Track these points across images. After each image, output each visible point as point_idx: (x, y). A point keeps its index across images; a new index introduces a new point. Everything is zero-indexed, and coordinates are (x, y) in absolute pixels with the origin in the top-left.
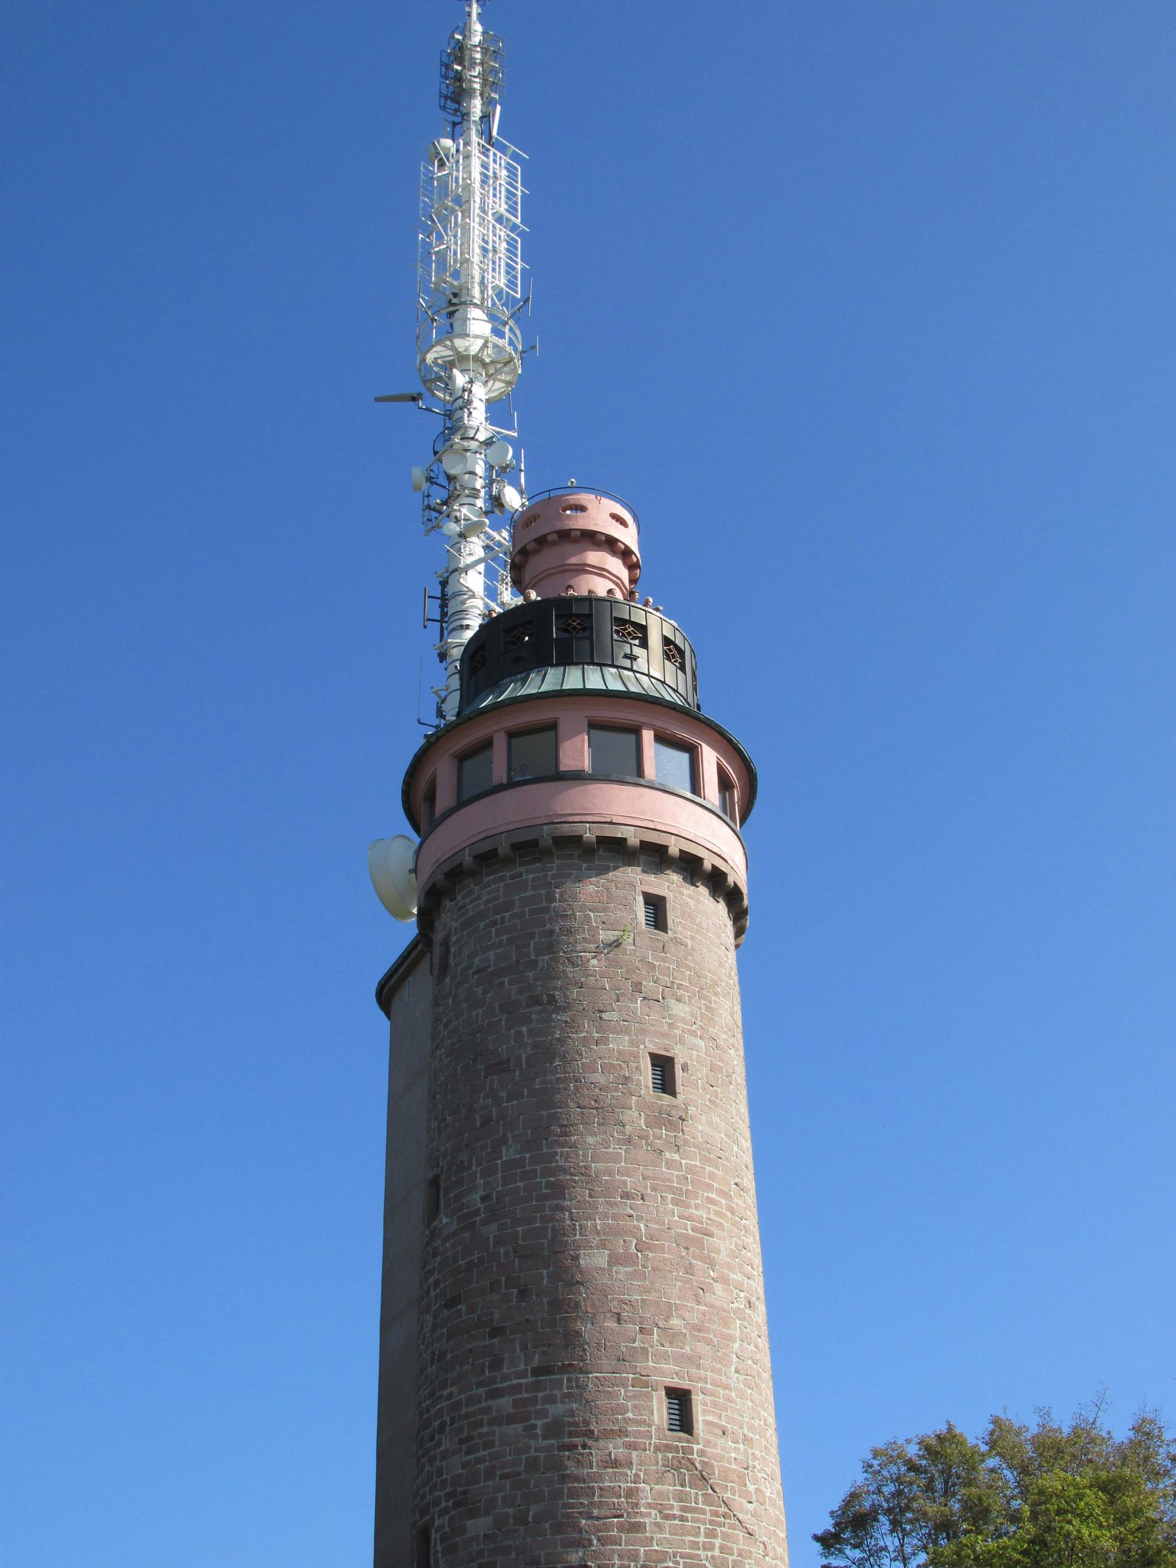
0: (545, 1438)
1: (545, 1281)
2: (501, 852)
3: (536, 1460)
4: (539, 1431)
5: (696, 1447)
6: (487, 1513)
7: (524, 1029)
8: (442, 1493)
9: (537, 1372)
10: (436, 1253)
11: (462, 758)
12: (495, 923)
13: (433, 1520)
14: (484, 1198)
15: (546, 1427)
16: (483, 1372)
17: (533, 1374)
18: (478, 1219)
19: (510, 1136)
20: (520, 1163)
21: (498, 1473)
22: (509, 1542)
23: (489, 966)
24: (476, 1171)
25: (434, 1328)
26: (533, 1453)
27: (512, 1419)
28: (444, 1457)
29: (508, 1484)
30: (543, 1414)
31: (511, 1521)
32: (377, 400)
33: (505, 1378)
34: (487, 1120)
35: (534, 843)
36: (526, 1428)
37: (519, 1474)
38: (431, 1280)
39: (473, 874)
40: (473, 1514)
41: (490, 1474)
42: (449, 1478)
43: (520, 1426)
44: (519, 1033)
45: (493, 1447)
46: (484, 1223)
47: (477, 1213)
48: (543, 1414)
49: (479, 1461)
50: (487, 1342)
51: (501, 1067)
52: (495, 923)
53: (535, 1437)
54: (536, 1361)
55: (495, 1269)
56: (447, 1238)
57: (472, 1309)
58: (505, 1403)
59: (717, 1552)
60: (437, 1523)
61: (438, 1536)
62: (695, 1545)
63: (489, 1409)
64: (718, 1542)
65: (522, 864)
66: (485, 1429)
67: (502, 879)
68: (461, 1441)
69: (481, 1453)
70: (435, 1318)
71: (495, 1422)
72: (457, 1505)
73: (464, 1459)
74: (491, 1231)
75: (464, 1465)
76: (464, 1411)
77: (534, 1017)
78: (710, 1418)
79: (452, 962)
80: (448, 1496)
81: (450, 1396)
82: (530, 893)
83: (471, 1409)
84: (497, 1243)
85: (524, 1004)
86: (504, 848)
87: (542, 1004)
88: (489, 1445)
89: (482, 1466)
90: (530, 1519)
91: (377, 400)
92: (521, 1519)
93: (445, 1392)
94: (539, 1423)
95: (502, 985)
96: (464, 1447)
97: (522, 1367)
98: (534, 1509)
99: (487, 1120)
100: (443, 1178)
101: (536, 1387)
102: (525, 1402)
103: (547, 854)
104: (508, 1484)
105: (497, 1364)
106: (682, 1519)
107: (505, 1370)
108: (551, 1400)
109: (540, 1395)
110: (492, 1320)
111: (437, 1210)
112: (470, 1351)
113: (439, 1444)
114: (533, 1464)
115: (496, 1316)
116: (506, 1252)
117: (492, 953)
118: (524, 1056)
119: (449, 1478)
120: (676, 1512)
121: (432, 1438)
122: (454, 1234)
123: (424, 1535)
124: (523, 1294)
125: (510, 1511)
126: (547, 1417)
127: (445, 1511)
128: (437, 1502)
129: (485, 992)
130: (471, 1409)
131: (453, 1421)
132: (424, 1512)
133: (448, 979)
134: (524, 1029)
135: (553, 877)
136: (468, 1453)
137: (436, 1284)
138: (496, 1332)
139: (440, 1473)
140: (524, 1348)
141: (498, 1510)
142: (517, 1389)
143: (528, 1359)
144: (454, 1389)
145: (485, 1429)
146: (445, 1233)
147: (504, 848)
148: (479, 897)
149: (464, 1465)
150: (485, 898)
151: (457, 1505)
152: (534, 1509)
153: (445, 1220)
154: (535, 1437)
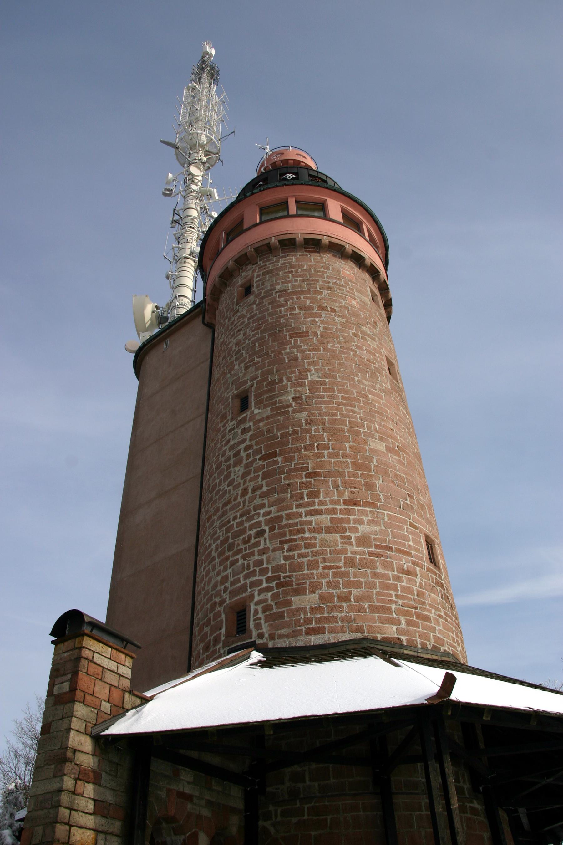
0: (358, 545)
7: (317, 320)
8: (263, 578)
10: (244, 431)
13: (252, 597)
14: (294, 399)
15: (358, 539)
16: (302, 498)
18: (290, 409)
21: (321, 565)
23: (289, 289)
24: (287, 384)
26: (349, 555)
27: (328, 530)
28: (263, 552)
30: (356, 530)
31: (336, 599)
32: (161, 141)
37: (340, 567)
40: (299, 591)
42: (270, 567)
43: (337, 536)
45: (315, 547)
46: (295, 411)
47: (290, 406)
48: (356, 530)
49: (301, 556)
53: (351, 544)
54: (346, 496)
55: (308, 438)
56: (262, 420)
58: (325, 519)
60: (257, 598)
61: (260, 608)
63: (310, 523)
66: (307, 535)
68: (282, 542)
69: (303, 551)
71: (318, 530)
72: (278, 586)
73: (285, 554)
75: (286, 558)
76: (284, 522)
81: (269, 513)
83: (291, 521)
87: (328, 311)
88: (307, 546)
89: (305, 560)
90: (352, 599)
91: (161, 141)
92: (345, 598)
94: (353, 536)
96: (286, 546)
97: (336, 498)
98: (355, 592)
101: (348, 512)
102: (341, 521)
105: (314, 494)
107: (322, 498)
108: (361, 522)
109: (352, 517)
110: (308, 467)
112: (289, 485)
113: (257, 544)
114: (350, 562)
116: (317, 430)
118: (318, 332)
119: (270, 567)
121: (246, 541)
122: (268, 418)
126: (358, 532)
128: (260, 582)
130: (291, 521)
131: (272, 529)
136: (289, 550)
138: (309, 475)
139: (260, 562)
142: (334, 511)
143: (340, 494)
145: (307, 535)
146: (258, 418)
149: (286, 558)
151: (278, 586)
152: (355, 592)
153: (256, 411)
154: (351, 544)
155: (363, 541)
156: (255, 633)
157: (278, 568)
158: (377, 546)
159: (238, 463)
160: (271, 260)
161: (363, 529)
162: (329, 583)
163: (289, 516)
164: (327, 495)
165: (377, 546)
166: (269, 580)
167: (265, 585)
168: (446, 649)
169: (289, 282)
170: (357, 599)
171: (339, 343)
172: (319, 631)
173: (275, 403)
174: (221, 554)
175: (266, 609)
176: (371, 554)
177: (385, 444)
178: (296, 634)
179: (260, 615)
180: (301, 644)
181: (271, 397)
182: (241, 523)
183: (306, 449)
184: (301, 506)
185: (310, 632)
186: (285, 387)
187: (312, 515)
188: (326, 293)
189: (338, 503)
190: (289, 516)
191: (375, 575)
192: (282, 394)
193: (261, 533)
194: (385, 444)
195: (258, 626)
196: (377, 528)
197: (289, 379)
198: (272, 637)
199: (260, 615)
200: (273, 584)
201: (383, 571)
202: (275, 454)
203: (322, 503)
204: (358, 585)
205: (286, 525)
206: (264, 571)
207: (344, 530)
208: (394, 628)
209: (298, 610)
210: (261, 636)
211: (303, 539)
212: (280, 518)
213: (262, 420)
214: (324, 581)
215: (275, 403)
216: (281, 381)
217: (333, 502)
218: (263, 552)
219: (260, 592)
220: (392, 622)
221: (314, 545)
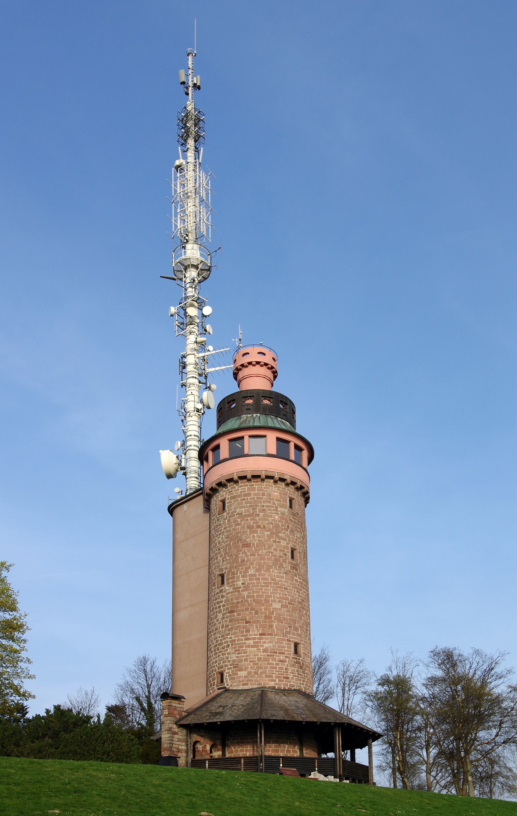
0: (263, 653)
1: (263, 610)
2: (248, 477)
3: (260, 658)
4: (261, 650)
5: (301, 658)
6: (245, 670)
7: (255, 535)
8: (229, 664)
9: (260, 635)
10: (223, 596)
11: (230, 440)
12: (244, 499)
13: (225, 670)
16: (243, 633)
17: (259, 635)
18: (240, 589)
19: (251, 567)
20: (255, 575)
21: (249, 660)
22: (252, 679)
23: (243, 513)
24: (240, 575)
25: (223, 618)
26: (259, 656)
27: (253, 646)
28: (229, 654)
29: (252, 663)
30: (262, 646)
31: (253, 673)
33: (251, 635)
34: (243, 561)
35: (259, 476)
36: (257, 649)
37: (255, 661)
38: (221, 604)
39: (236, 482)
40: (240, 670)
41: (246, 660)
42: (231, 660)
44: (253, 536)
45: (247, 653)
46: (243, 591)
47: (240, 587)
48: (262, 646)
49: (242, 656)
50: (244, 625)
51: (248, 545)
52: (244, 499)
54: (260, 632)
55: (247, 605)
56: (229, 593)
57: (239, 615)
58: (251, 642)
59: (305, 686)
60: (227, 671)
61: (227, 675)
62: (300, 684)
63: (245, 643)
64: (305, 683)
65: (253, 482)
67: (246, 485)
68: (235, 651)
69: (243, 654)
70: (223, 615)
71: (249, 646)
72: (234, 667)
73: (236, 655)
74: (246, 594)
75: (237, 657)
77: (258, 532)
78: (304, 651)
79: (226, 508)
80: (230, 665)
81: (231, 638)
82: (256, 492)
83: (239, 642)
84: (248, 596)
85: (255, 527)
86: (249, 476)
87: (261, 528)
89: (243, 658)
90: (259, 673)
93: (229, 637)
94: (261, 648)
95: (247, 520)
96: (237, 652)
97: (256, 633)
99: (243, 561)
100: (225, 575)
101: (260, 639)
102: (257, 642)
103: (263, 480)
104: (252, 663)
105: (248, 631)
106: (298, 677)
107: (251, 633)
108: (265, 643)
109: (262, 641)
110: (246, 619)
111: (223, 583)
112: (239, 626)
113: (227, 650)
114: (260, 659)
115: (247, 618)
116: (251, 600)
117: (243, 509)
118: (255, 543)
119: (231, 660)
120: (296, 675)
122: (231, 592)
123: (222, 674)
124: (256, 613)
125: (253, 671)
126: (264, 647)
127: (230, 668)
128: (227, 666)
129: (241, 521)
130: (239, 642)
131: (232, 645)
132: (222, 667)
133: (225, 514)
134: (255, 535)
135: (264, 488)
136: (238, 654)
137: (224, 606)
138: (247, 622)
139: (227, 658)
140: (257, 627)
141: (249, 670)
142: (255, 638)
143: (258, 631)
144: (233, 636)
145: (244, 648)
146: (227, 591)
147: (249, 476)
148: (238, 490)
149: (237, 657)
150: (240, 490)
153: (227, 588)
154: (260, 652)
155: (265, 651)
156: (226, 684)
157: (234, 661)
158: (271, 652)
159: (220, 612)
160: (234, 488)
161: (266, 645)
162: (251, 667)
163: (238, 640)
164: (253, 631)
165: (271, 652)
166: (230, 665)
167: (229, 667)
168: (295, 688)
169: (244, 507)
170: (261, 673)
171: (265, 549)
172: (247, 684)
173: (234, 585)
174: (215, 651)
175: (230, 676)
176: (268, 656)
177: (280, 604)
178: (239, 685)
179: (228, 678)
180: (240, 689)
181: (232, 582)
182: (221, 640)
183: (246, 610)
184: (243, 636)
185: (243, 685)
186: (238, 577)
187: (247, 640)
188: (261, 514)
189: (256, 635)
190: (238, 640)
191: (268, 664)
192: (237, 581)
193: (228, 646)
194: (280, 604)
195: (227, 682)
196: (272, 645)
197: (241, 573)
198: (231, 686)
199: (228, 678)
200: (232, 667)
201: (272, 662)
202: (233, 612)
203: (251, 635)
204: (261, 668)
205: (238, 644)
206: (229, 661)
207: (258, 647)
208: (274, 683)
209: (240, 677)
210: (228, 685)
211: (243, 650)
212: (235, 640)
213: (229, 593)
214: (249, 666)
215: (234, 585)
216: (237, 573)
217: (255, 635)
218: (229, 654)
219: (228, 669)
220: (272, 681)
221: (246, 652)
